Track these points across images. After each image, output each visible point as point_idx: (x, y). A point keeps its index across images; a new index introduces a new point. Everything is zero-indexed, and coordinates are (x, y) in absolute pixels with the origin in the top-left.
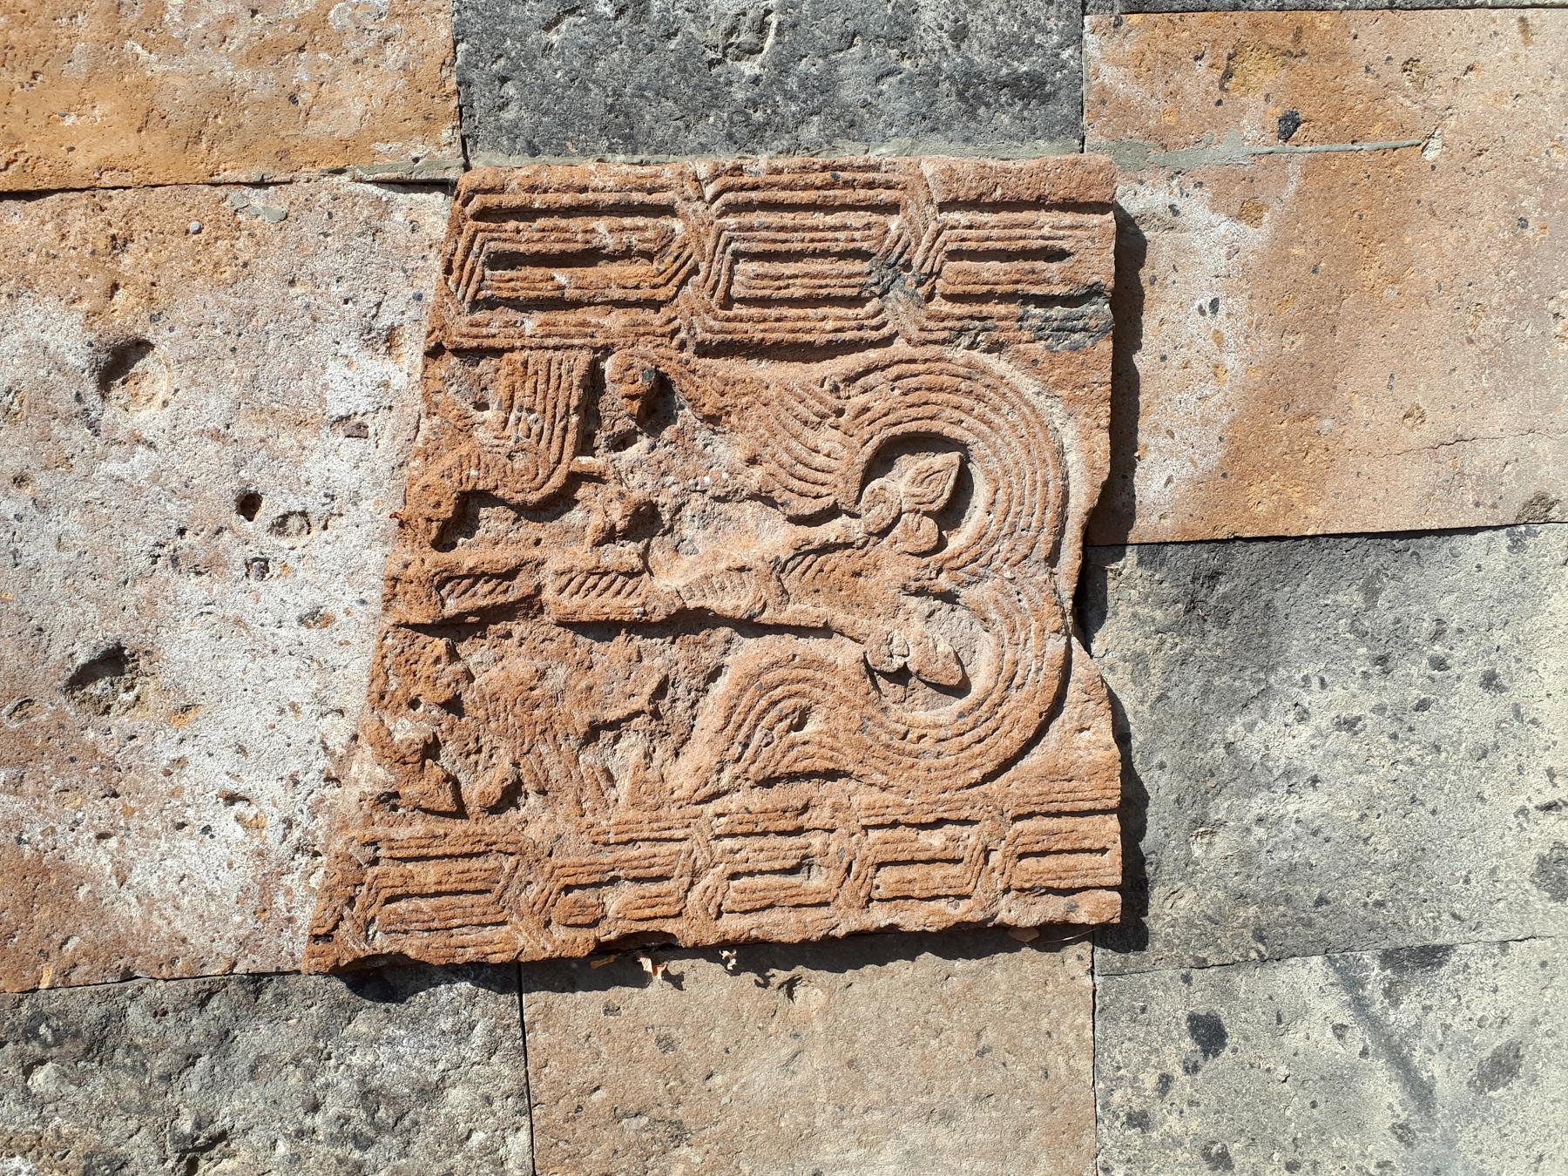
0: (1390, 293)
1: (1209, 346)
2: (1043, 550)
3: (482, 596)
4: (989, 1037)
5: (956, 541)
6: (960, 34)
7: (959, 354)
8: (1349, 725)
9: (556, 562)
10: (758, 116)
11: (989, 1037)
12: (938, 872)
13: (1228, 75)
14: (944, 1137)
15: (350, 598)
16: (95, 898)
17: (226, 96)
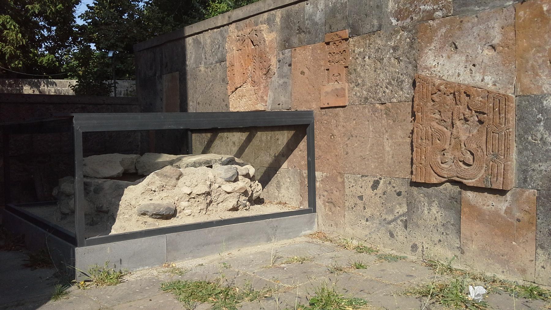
0: (493, 233)
1: (487, 204)
2: (458, 175)
3: (457, 97)
4: (401, 164)
5: (461, 164)
6: (533, 170)
7: (485, 165)
8: (436, 219)
9: (461, 107)
10: (523, 139)
11: (401, 164)
12: (419, 157)
13: (526, 211)
14: (390, 156)
15: (461, 79)
16: (428, 46)
17: (527, 62)
